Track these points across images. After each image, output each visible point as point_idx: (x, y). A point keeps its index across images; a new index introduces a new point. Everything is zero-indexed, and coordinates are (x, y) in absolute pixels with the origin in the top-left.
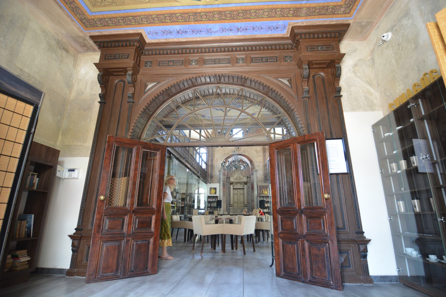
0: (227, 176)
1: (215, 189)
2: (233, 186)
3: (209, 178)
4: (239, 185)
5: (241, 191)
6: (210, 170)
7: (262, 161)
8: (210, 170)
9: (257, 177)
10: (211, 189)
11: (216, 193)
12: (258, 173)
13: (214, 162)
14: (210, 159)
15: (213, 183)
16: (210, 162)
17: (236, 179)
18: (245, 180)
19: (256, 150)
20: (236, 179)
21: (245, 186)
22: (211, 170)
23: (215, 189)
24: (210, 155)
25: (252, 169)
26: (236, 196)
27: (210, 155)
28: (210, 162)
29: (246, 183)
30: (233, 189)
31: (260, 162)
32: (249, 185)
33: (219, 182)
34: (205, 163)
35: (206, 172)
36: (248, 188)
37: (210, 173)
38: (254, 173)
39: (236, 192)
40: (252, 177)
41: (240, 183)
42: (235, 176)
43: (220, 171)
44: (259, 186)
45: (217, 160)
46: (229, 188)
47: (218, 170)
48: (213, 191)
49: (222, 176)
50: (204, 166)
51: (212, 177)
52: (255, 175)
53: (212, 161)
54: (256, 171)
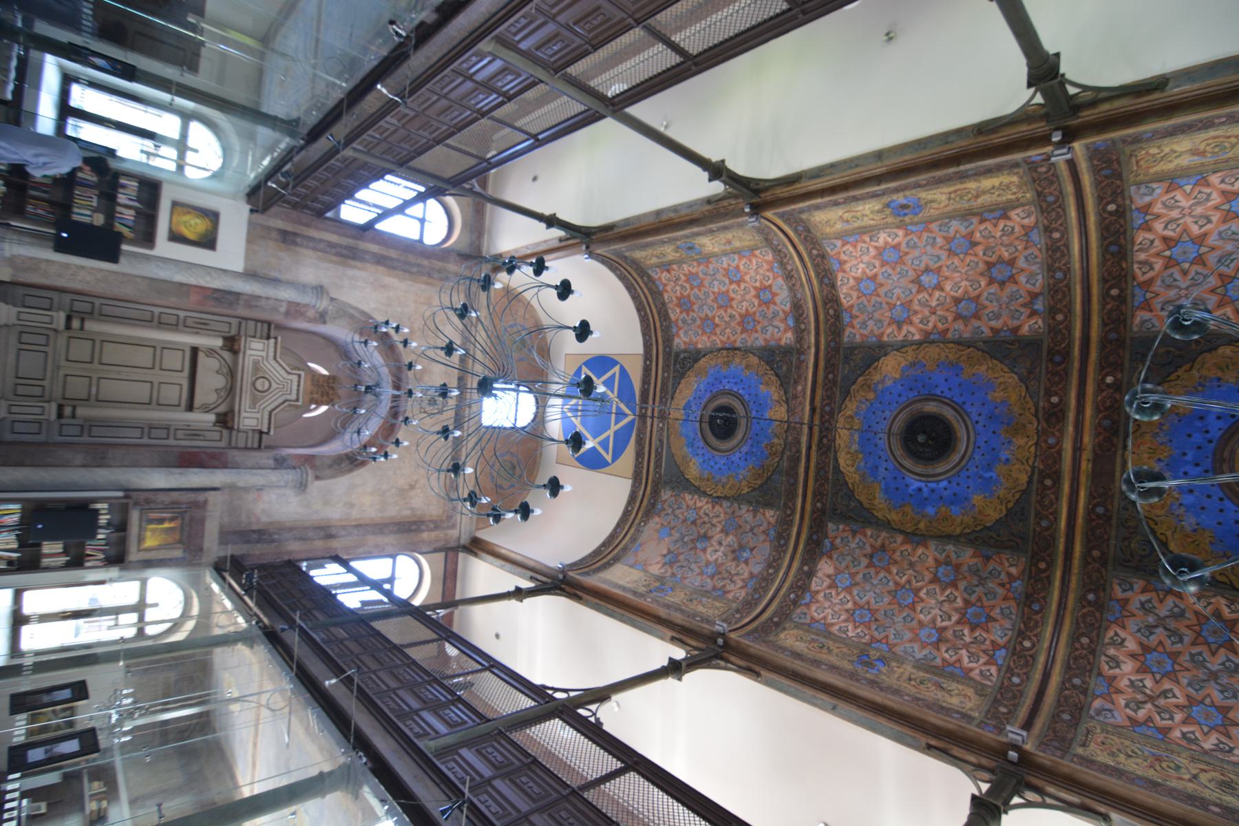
0: (280, 327)
1: (208, 242)
2: (211, 352)
3: (280, 224)
4: (220, 382)
5: (174, 392)
6: (334, 238)
7: (355, 514)
8: (334, 238)
9: (260, 489)
10: (213, 216)
11: (176, 237)
12: (290, 492)
13: (371, 268)
14: (393, 254)
15: (250, 240)
16: (374, 248)
17: (256, 363)
18: (249, 419)
19: (412, 487)
20: (256, 367)
21: (211, 417)
22: (331, 245)
23: (208, 242)
24: (411, 258)
25: (309, 459)
26: (144, 356)
27: (411, 258)
28: (374, 248)
29: (225, 420)
30: (195, 351)
31: (352, 505)
32: (215, 440)
33: (250, 274)
34: (370, 226)
35: (320, 214)
36: (194, 433)
37: (313, 233)
38: (289, 476)
39: (175, 361)
40: (264, 457)
41: (231, 391)
42: (276, 371)
43: (320, 290)
44: (201, 497)
45: (384, 286)
46: (200, 327)
47: (325, 281)
48: (194, 226)
49: (286, 294)
50: (351, 212)
51: (288, 238)
52: (274, 476)
53: (380, 260)
54: (302, 487)
